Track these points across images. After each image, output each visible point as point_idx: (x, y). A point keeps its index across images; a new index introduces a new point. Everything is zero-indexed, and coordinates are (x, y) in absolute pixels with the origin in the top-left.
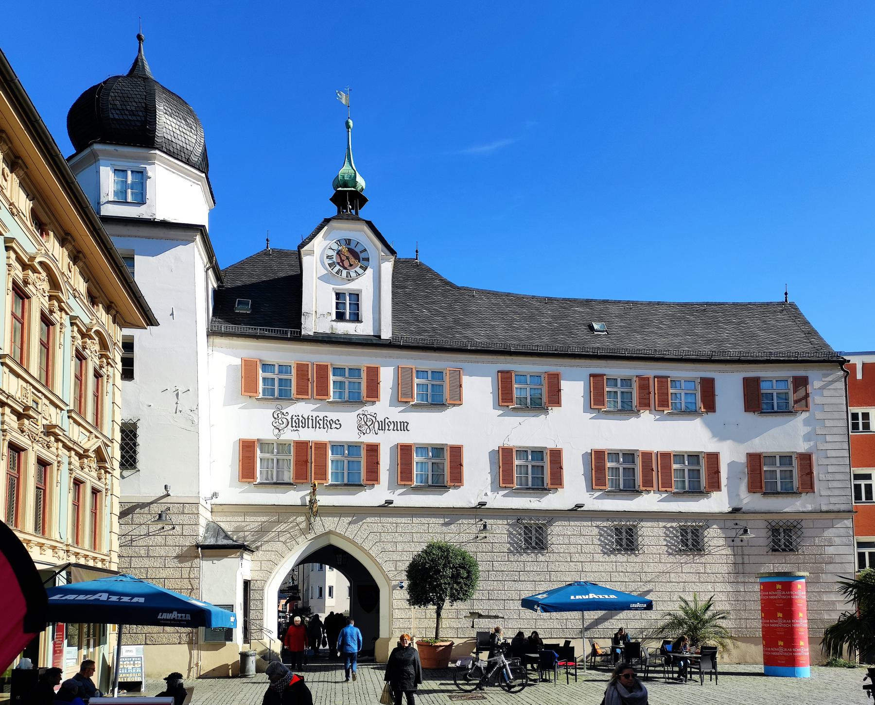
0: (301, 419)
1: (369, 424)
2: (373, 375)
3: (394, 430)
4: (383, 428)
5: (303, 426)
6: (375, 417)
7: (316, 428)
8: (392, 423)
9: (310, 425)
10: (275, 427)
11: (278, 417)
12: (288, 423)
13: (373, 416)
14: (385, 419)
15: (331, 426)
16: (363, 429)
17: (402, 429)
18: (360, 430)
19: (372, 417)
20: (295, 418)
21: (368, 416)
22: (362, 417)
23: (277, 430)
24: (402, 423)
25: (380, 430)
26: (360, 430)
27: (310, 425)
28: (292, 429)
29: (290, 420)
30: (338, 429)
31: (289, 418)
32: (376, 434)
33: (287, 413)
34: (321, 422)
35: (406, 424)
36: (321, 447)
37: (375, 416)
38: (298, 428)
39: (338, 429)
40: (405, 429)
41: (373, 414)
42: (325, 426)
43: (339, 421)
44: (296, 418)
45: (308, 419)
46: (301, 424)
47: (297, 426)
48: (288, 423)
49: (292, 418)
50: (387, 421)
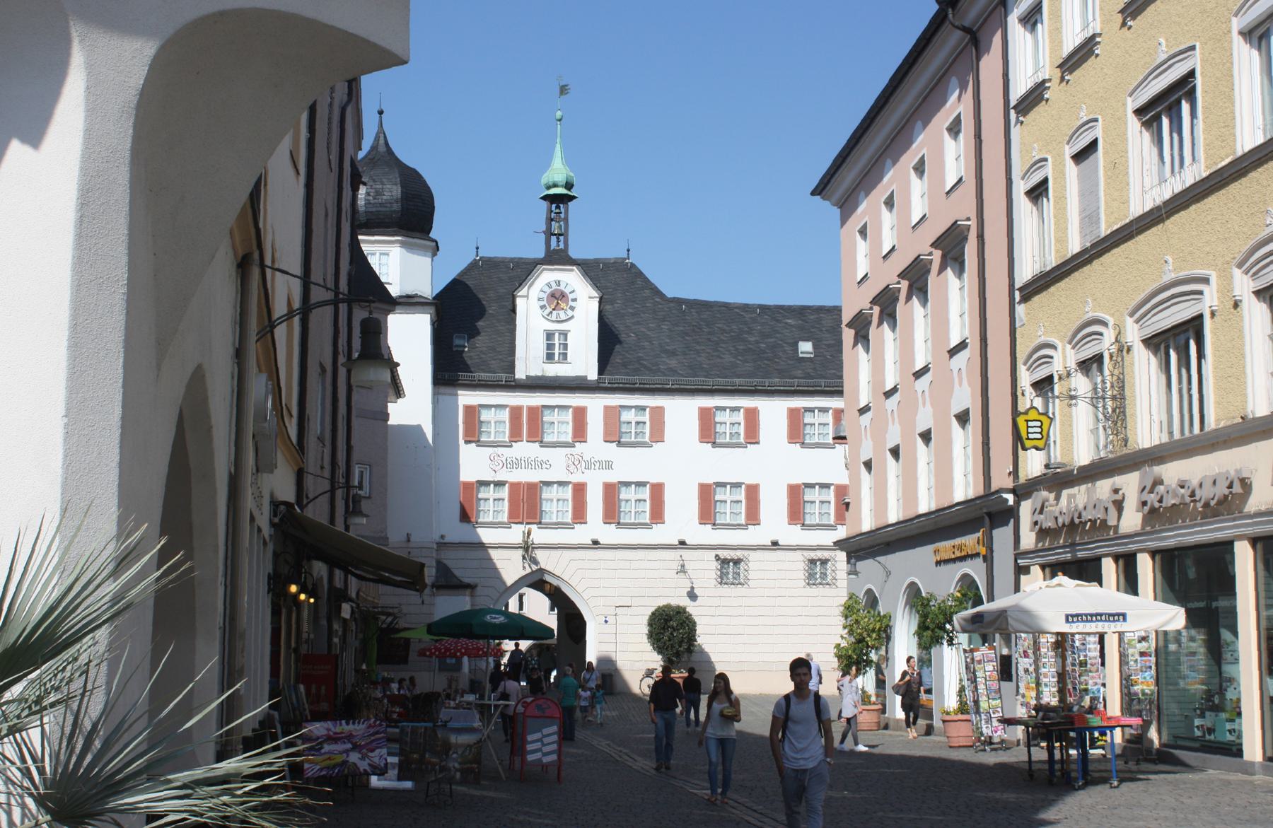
0: (514, 460)
2: (580, 416)
9: (523, 466)
20: (509, 460)
22: (570, 457)
27: (523, 466)
34: (533, 463)
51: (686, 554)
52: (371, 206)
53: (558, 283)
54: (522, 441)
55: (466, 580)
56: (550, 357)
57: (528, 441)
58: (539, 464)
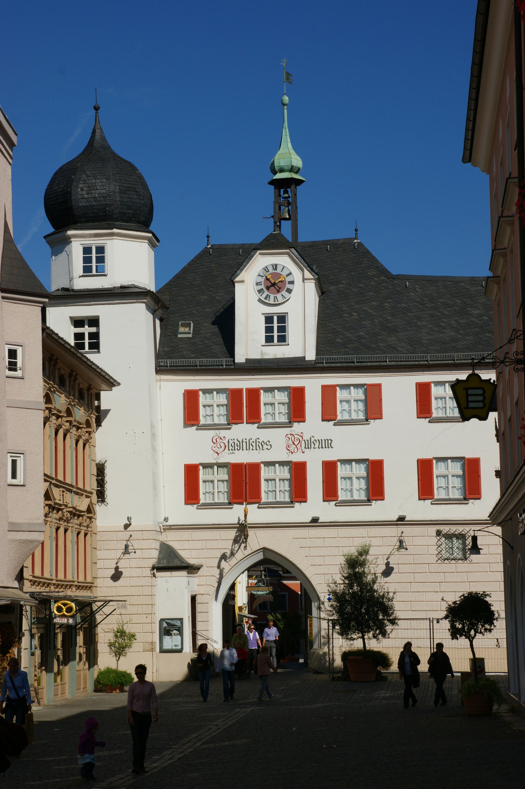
0: (236, 442)
1: (296, 443)
3: (319, 448)
4: (309, 447)
5: (239, 448)
6: (302, 436)
7: (249, 449)
8: (317, 441)
9: (244, 448)
10: (214, 451)
11: (217, 442)
12: (225, 447)
13: (300, 436)
14: (310, 438)
15: (263, 447)
16: (291, 448)
17: (327, 446)
18: (289, 450)
19: (299, 437)
20: (231, 442)
21: (296, 436)
22: (290, 437)
23: (216, 454)
24: (327, 441)
25: (306, 448)
26: (289, 450)
27: (244, 448)
28: (229, 452)
29: (227, 444)
30: (268, 449)
31: (226, 442)
32: (303, 452)
33: (224, 437)
34: (254, 444)
35: (330, 441)
36: (255, 468)
37: (301, 435)
38: (234, 451)
39: (268, 449)
40: (329, 446)
41: (300, 434)
42: (258, 448)
43: (269, 442)
44: (232, 441)
45: (242, 442)
46: (236, 447)
47: (233, 449)
48: (225, 447)
49: (229, 442)
50: (313, 439)
51: (408, 530)
52: (85, 200)
53: (275, 267)
54: (243, 423)
55: (192, 561)
56: (269, 339)
57: (247, 423)
58: (260, 445)
